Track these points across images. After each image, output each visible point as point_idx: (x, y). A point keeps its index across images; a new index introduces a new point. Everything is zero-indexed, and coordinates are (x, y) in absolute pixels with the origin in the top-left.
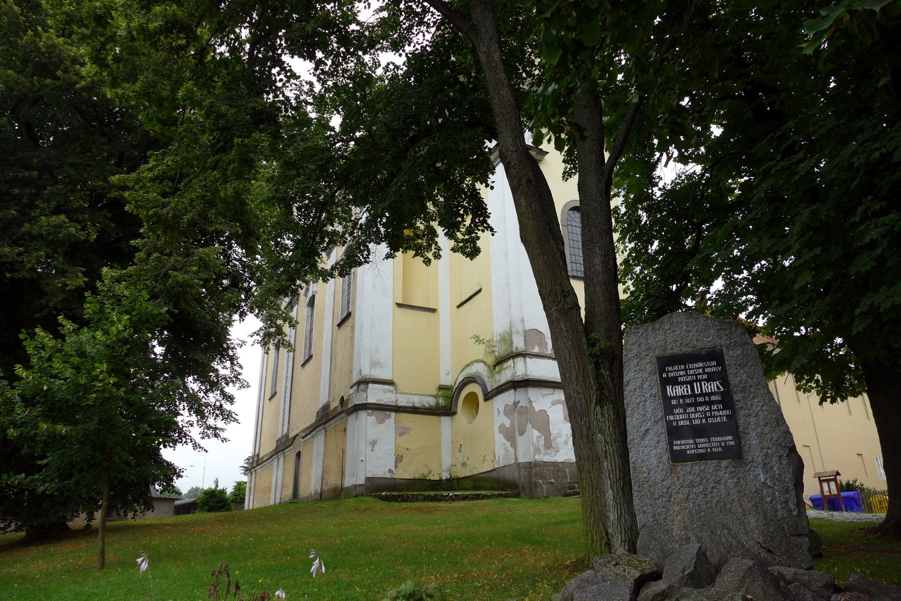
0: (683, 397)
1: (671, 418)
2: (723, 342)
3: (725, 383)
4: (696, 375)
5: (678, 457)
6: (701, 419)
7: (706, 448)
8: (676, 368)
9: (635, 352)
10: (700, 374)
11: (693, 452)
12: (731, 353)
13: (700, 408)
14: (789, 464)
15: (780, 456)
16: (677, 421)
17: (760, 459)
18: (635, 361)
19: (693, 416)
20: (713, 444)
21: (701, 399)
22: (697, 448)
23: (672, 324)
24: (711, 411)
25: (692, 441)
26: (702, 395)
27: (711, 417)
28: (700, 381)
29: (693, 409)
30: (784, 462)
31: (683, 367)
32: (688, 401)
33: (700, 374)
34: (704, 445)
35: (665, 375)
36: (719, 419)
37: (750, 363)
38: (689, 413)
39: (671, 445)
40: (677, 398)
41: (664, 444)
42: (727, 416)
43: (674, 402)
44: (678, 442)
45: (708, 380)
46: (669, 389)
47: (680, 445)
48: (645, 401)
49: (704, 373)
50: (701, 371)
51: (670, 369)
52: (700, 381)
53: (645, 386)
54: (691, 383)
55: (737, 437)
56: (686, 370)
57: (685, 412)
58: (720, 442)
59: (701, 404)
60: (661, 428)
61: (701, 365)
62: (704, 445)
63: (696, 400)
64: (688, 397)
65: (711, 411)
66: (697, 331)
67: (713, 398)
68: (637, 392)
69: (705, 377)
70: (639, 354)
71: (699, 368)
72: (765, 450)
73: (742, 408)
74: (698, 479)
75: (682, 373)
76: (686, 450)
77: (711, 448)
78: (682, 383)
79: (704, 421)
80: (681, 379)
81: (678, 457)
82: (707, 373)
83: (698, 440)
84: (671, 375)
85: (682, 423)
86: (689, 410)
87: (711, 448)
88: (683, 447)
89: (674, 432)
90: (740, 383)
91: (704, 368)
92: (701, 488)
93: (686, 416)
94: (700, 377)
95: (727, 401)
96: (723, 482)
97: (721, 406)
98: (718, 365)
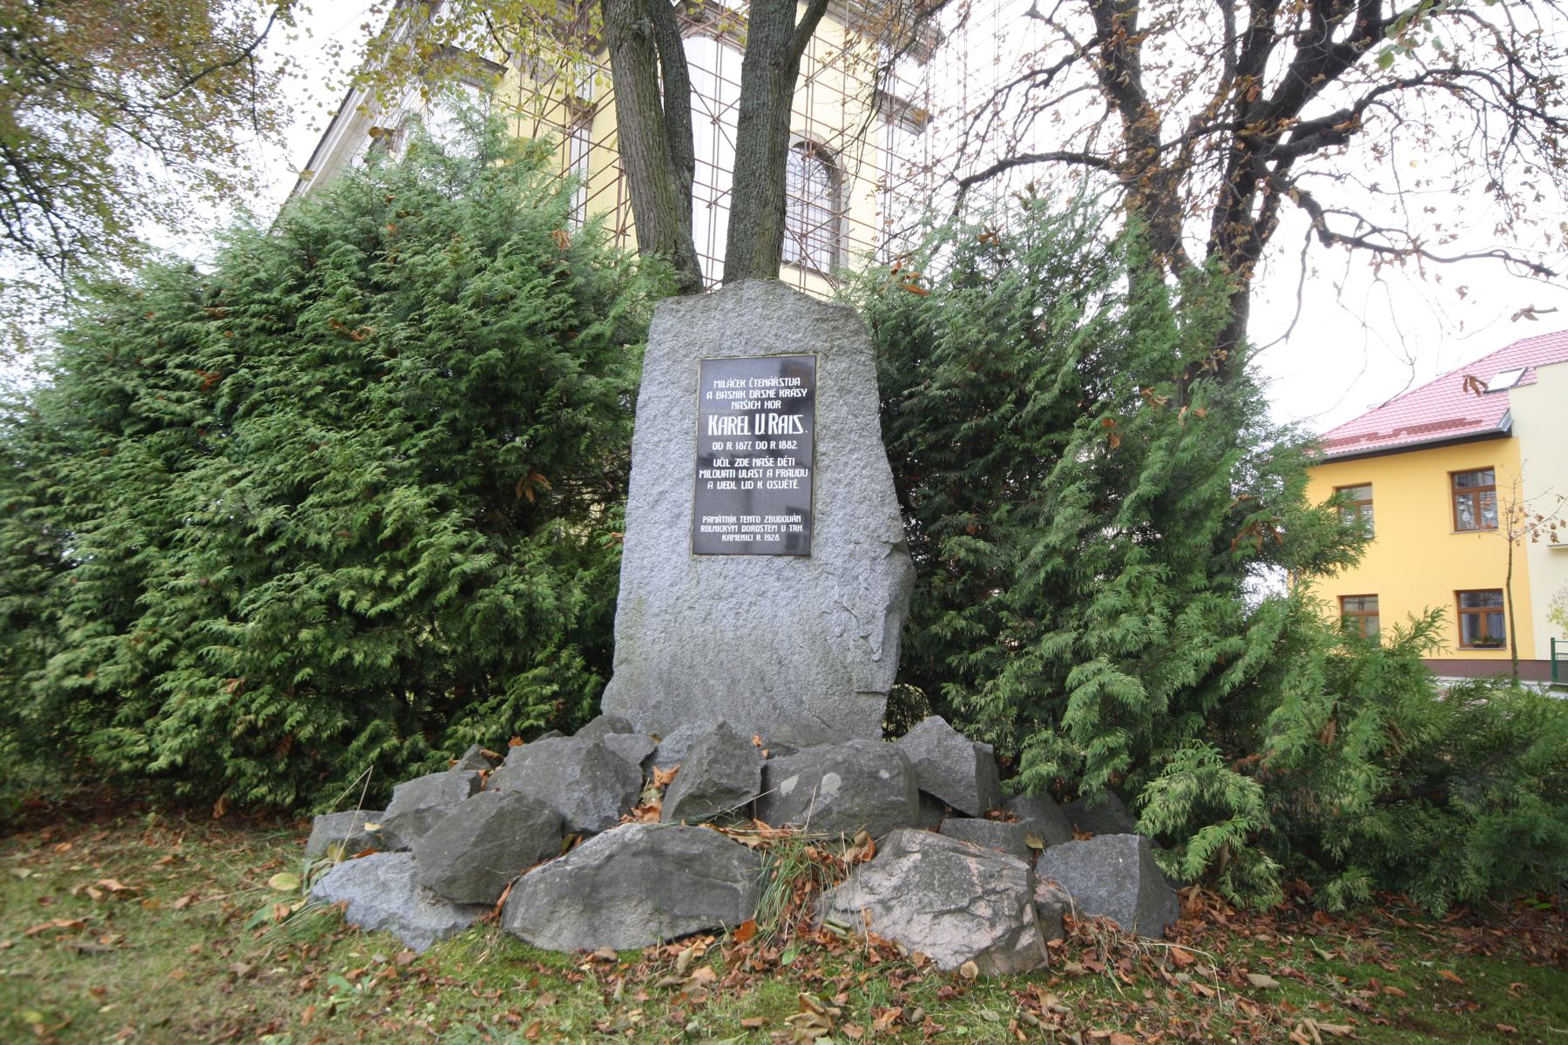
0: (734, 439)
1: (706, 473)
2: (819, 345)
3: (809, 421)
4: (763, 401)
5: (702, 547)
7: (755, 534)
8: (731, 384)
9: (666, 348)
10: (769, 399)
11: (731, 538)
12: (829, 366)
13: (757, 462)
14: (887, 573)
15: (875, 559)
16: (715, 480)
18: (665, 364)
19: (743, 474)
20: (768, 528)
21: (761, 445)
22: (739, 532)
23: (739, 301)
24: (775, 467)
25: (733, 519)
26: (765, 437)
27: (774, 478)
28: (767, 412)
29: (746, 462)
30: (880, 569)
31: (743, 383)
32: (741, 446)
33: (769, 399)
34: (752, 528)
35: (709, 396)
36: (785, 483)
37: (858, 389)
38: (737, 469)
39: (696, 522)
40: (723, 439)
41: (686, 522)
42: (800, 480)
43: (717, 446)
44: (710, 519)
45: (780, 412)
46: (712, 421)
47: (715, 524)
48: (669, 440)
49: (777, 397)
51: (721, 384)
52: (767, 412)
53: (674, 412)
55: (809, 520)
56: (747, 389)
58: (779, 525)
59: (760, 454)
60: (686, 493)
62: (752, 528)
63: (753, 446)
64: (742, 438)
65: (775, 467)
66: (779, 318)
67: (783, 445)
68: (658, 421)
69: (778, 404)
70: (673, 351)
71: (770, 388)
72: (852, 546)
74: (732, 585)
75: (741, 394)
76: (721, 534)
77: (762, 535)
79: (760, 484)
81: (702, 547)
82: (782, 399)
83: (744, 518)
84: (720, 395)
85: (722, 486)
86: (740, 462)
87: (762, 535)
88: (717, 529)
89: (705, 501)
90: (834, 422)
92: (734, 601)
93: (732, 473)
94: (769, 405)
95: (808, 459)
96: (770, 594)
97: (792, 460)
98: (802, 386)
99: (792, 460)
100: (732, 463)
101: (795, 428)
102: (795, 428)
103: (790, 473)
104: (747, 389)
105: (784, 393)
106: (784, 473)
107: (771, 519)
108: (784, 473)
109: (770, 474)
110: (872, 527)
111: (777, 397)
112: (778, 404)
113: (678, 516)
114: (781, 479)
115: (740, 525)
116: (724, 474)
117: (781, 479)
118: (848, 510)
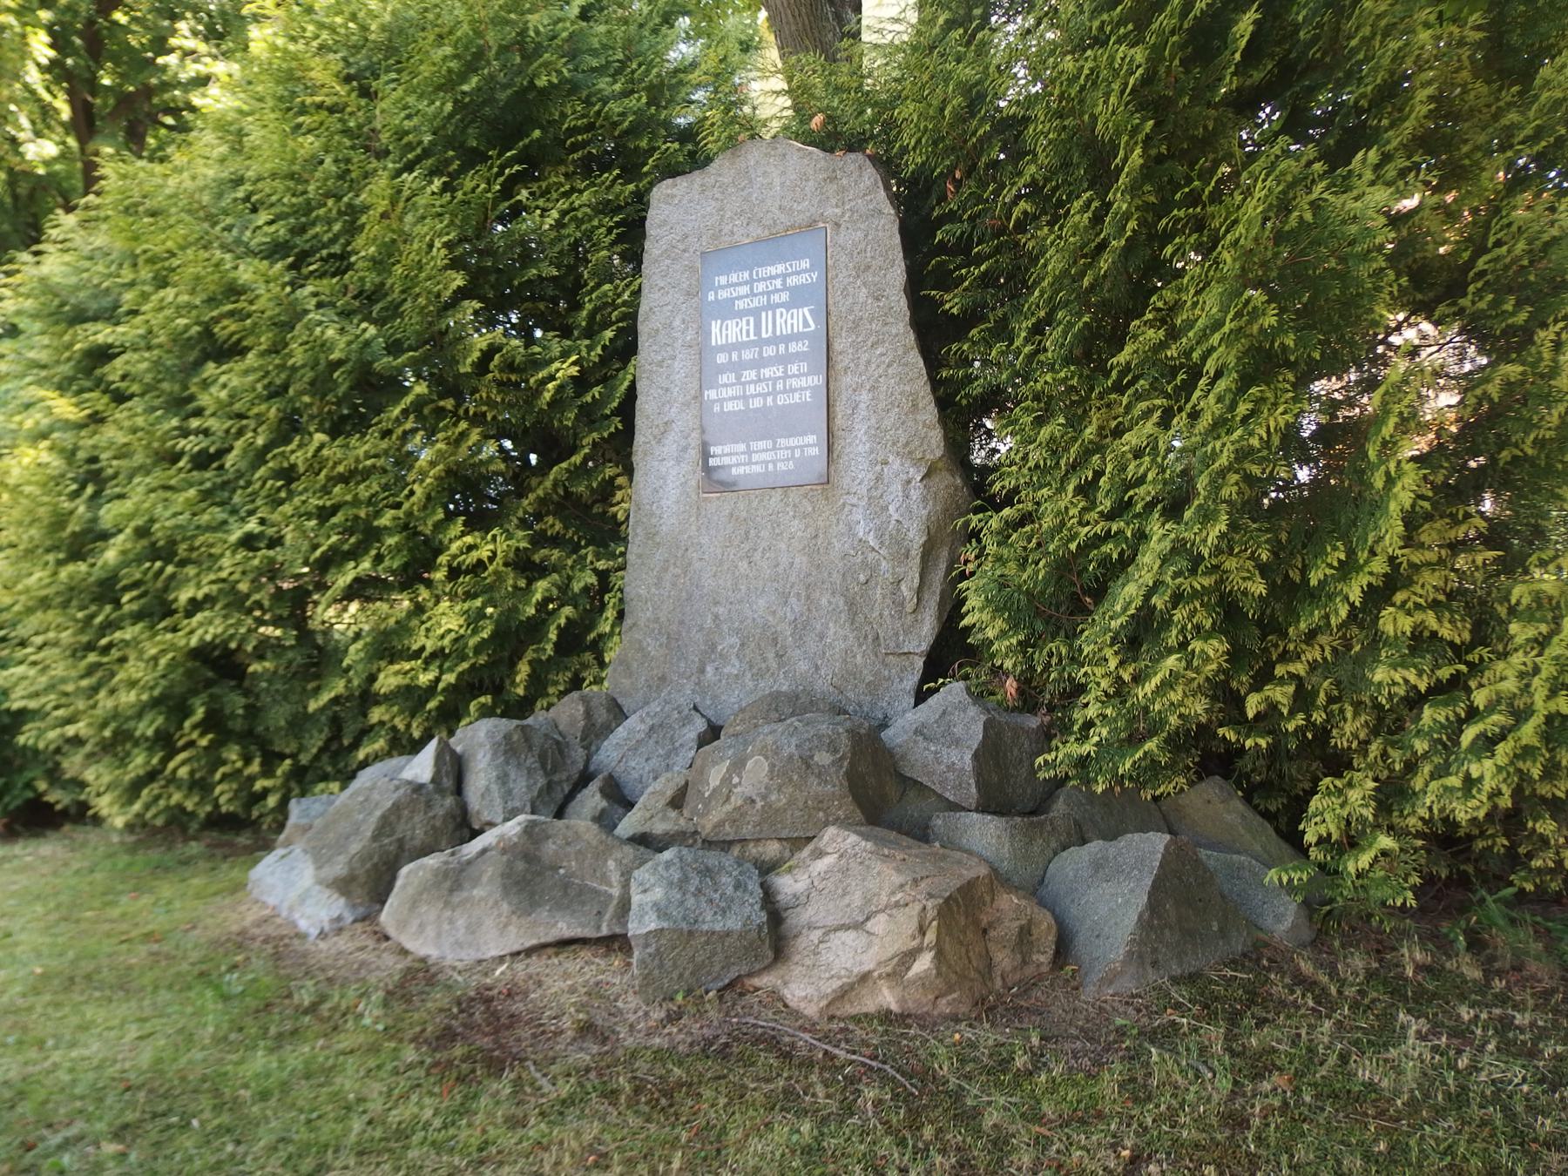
0: (739, 346)
4: (769, 293)
6: (764, 396)
8: (734, 278)
10: (777, 291)
13: (767, 372)
16: (721, 401)
17: (863, 490)
19: (751, 390)
20: (781, 454)
21: (769, 351)
22: (750, 463)
24: (786, 376)
25: (742, 447)
26: (775, 340)
27: (785, 391)
28: (772, 307)
30: (915, 494)
31: (746, 275)
32: (747, 355)
33: (777, 291)
34: (764, 456)
35: (711, 297)
36: (797, 395)
38: (744, 384)
40: (728, 348)
42: (814, 389)
45: (788, 306)
46: (715, 327)
48: (673, 358)
49: (785, 288)
50: (778, 283)
51: (723, 280)
54: (756, 313)
57: (739, 382)
58: (792, 449)
61: (780, 268)
62: (764, 456)
69: (785, 297)
72: (878, 468)
73: (846, 369)
75: (744, 290)
76: (730, 467)
77: (774, 462)
78: (741, 314)
79: (769, 399)
80: (741, 305)
83: (754, 445)
84: (723, 295)
85: (729, 407)
86: (750, 375)
90: (851, 311)
91: (784, 276)
94: (776, 298)
97: (804, 367)
99: (804, 367)
100: (738, 377)
101: (806, 324)
102: (806, 324)
103: (803, 382)
104: (750, 282)
105: (792, 281)
106: (795, 383)
107: (782, 442)
108: (795, 383)
109: (780, 386)
110: (903, 440)
111: (785, 288)
112: (785, 297)
113: (685, 449)
114: (793, 391)
115: (749, 452)
116: (730, 392)
117: (793, 391)
118: (873, 421)
